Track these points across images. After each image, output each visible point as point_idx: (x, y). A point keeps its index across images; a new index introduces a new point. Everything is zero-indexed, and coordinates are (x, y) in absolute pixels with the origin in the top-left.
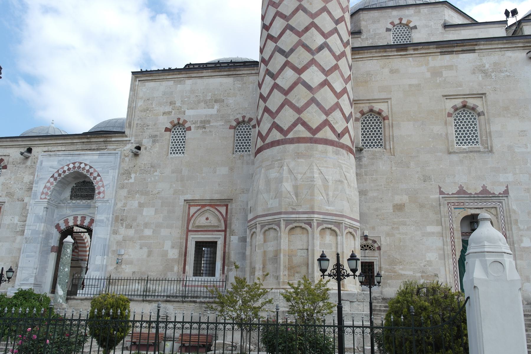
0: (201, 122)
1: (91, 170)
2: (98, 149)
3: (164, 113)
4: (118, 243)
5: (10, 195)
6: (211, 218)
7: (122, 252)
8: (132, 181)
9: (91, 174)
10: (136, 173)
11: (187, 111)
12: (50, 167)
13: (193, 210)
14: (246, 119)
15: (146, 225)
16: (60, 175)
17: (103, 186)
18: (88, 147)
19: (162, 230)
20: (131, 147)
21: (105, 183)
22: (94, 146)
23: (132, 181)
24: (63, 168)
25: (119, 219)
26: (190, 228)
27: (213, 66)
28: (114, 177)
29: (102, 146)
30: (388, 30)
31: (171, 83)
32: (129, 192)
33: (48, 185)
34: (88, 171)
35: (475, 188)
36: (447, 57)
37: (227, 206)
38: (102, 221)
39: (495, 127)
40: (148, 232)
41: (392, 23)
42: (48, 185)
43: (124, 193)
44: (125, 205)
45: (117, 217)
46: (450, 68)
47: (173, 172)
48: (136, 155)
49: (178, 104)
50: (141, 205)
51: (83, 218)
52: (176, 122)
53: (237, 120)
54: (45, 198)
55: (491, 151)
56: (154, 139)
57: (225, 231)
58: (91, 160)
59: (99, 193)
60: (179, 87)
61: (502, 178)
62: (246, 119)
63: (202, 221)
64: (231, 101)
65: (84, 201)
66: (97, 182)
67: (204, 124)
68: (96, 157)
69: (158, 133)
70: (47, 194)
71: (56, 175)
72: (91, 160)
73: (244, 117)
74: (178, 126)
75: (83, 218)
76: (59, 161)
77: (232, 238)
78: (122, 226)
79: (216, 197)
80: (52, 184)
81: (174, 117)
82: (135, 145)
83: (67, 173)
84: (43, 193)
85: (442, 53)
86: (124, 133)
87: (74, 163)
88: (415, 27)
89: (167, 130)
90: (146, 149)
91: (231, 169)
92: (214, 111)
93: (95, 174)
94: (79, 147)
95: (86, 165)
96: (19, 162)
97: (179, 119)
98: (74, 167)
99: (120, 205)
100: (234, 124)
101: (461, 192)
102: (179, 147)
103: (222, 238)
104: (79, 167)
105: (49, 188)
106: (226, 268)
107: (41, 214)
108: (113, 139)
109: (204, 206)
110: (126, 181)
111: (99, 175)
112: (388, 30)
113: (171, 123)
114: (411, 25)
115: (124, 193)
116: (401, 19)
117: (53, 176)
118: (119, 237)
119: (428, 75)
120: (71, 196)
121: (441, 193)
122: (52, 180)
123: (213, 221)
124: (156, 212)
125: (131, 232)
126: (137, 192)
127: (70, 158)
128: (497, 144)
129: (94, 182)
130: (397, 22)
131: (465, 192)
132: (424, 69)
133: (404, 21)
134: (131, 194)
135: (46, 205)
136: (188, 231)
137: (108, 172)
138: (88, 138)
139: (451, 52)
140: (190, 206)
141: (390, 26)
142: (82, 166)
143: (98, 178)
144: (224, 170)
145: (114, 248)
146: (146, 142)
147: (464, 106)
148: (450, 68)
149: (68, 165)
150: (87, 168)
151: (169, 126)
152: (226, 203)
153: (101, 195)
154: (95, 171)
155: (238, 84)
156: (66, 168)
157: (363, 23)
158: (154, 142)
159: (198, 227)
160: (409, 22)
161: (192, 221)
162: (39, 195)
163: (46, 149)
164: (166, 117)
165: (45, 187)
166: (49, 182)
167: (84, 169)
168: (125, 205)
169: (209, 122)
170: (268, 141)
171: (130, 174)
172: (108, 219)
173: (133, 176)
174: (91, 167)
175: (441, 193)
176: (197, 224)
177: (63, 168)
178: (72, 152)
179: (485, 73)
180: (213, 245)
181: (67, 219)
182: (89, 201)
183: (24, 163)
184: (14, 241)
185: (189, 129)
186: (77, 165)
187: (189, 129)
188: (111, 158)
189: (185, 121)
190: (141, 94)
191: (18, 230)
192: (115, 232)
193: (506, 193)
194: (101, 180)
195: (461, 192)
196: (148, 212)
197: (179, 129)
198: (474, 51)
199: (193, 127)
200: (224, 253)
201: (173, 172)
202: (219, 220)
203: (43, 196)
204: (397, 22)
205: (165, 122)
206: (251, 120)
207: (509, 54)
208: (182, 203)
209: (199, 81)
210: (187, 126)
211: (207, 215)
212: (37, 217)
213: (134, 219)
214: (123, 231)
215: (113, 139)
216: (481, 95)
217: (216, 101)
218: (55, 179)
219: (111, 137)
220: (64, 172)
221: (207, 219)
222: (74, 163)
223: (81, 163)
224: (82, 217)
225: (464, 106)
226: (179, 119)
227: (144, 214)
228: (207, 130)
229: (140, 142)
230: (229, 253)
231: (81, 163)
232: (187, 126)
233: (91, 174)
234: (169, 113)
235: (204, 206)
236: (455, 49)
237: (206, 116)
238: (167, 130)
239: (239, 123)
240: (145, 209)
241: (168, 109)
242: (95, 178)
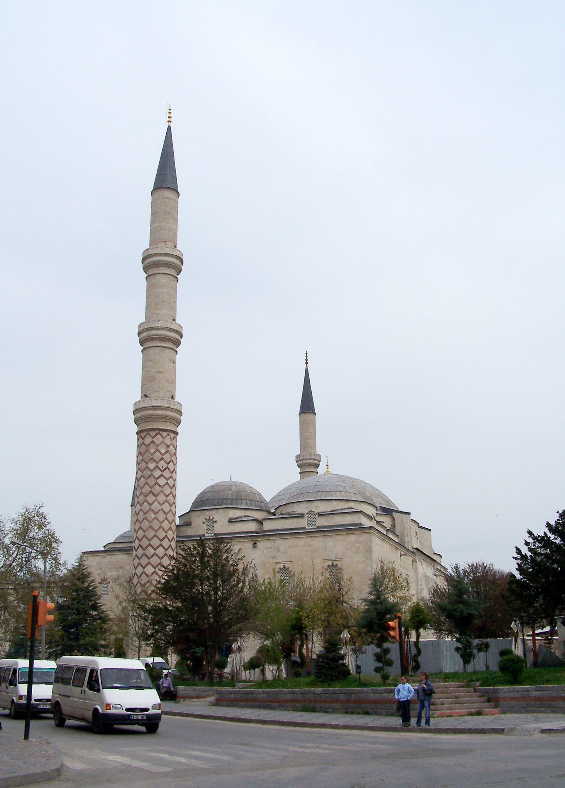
30: (204, 523)
41: (206, 519)
49: (104, 570)
60: (104, 560)
81: (102, 576)
88: (216, 522)
112: (204, 523)
114: (214, 520)
116: (210, 517)
130: (208, 518)
133: (211, 518)
141: (205, 521)
151: (100, 581)
157: (193, 518)
160: (213, 518)
187: (109, 583)
189: (107, 579)
199: (111, 582)
204: (208, 518)
207: (245, 544)
209: (113, 557)
210: (108, 581)
217: (121, 568)
232: (108, 581)
241: (99, 572)
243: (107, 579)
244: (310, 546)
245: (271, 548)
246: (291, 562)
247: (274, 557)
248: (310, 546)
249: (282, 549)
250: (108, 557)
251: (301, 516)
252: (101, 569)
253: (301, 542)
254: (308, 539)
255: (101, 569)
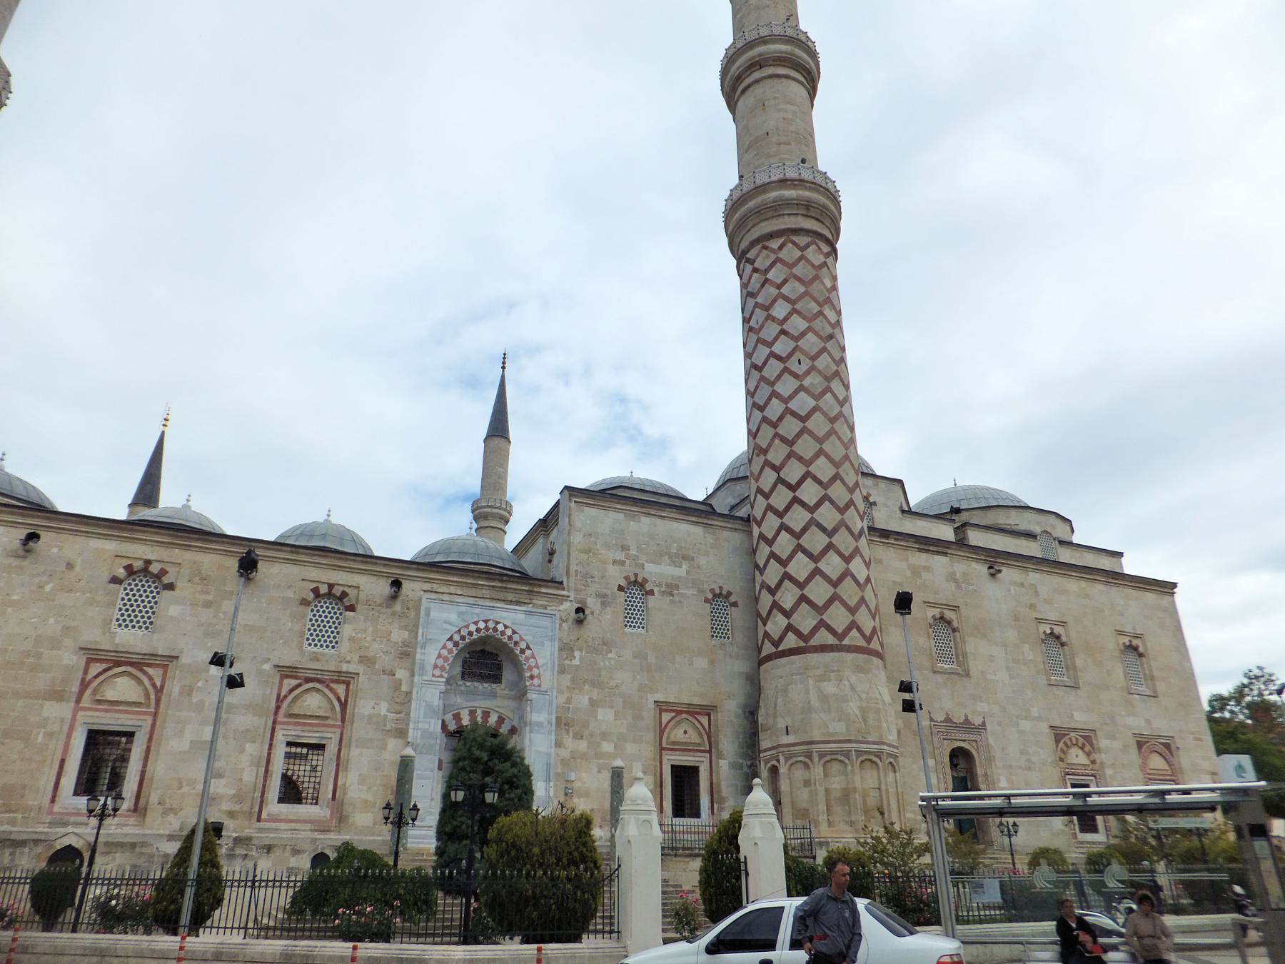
0: (667, 585)
1: (516, 638)
2: (518, 603)
3: (614, 562)
4: (564, 762)
5: (366, 660)
6: (690, 731)
7: (573, 776)
8: (576, 662)
9: (516, 643)
10: (581, 650)
11: (647, 565)
12: (446, 622)
13: (666, 717)
14: (724, 592)
15: (604, 736)
16: (463, 638)
17: (537, 666)
18: (501, 596)
19: (627, 745)
20: (568, 607)
21: (540, 662)
22: (511, 597)
23: (576, 662)
24: (467, 626)
25: (563, 723)
26: (664, 745)
27: (677, 503)
28: (552, 654)
29: (525, 598)
31: (621, 516)
32: (573, 680)
33: (445, 652)
34: (510, 638)
35: (959, 718)
36: (924, 555)
37: (709, 715)
38: (540, 725)
39: (969, 648)
40: (607, 747)
42: (445, 652)
43: (566, 680)
44: (569, 701)
45: (558, 719)
46: (927, 569)
47: (635, 657)
48: (580, 622)
49: (633, 551)
50: (593, 703)
51: (486, 714)
52: (633, 579)
53: (712, 590)
54: (441, 676)
55: (968, 675)
56: (604, 599)
57: (710, 752)
58: (511, 619)
59: (532, 677)
61: (983, 707)
62: (724, 592)
63: (678, 734)
64: (703, 561)
65: (486, 685)
66: (527, 659)
67: (671, 589)
68: (521, 617)
69: (609, 592)
70: (443, 668)
71: (457, 638)
72: (511, 619)
73: (721, 588)
74: (637, 585)
75: (486, 714)
76: (460, 614)
77: (722, 762)
78: (568, 731)
79: (696, 701)
80: (450, 651)
81: (629, 570)
82: (577, 605)
83: (475, 636)
84: (436, 666)
85: (920, 550)
86: (561, 583)
87: (486, 621)
89: (621, 588)
90: (592, 613)
91: (712, 662)
92: (682, 572)
93: (523, 645)
94: (486, 593)
95: (506, 627)
96: (379, 602)
97: (636, 575)
98: (487, 628)
99: (562, 699)
100: (710, 596)
101: (948, 720)
102: (632, 618)
103: (707, 761)
104: (495, 630)
105: (446, 659)
106: (716, 806)
107: (436, 703)
108: (543, 590)
109: (679, 713)
110: (567, 662)
111: (528, 648)
113: (626, 578)
115: (566, 680)
117: (451, 639)
118: (565, 753)
119: (909, 573)
120: (463, 673)
121: (932, 720)
122: (450, 645)
123: (693, 737)
124: (617, 716)
125: (582, 746)
126: (585, 681)
127: (477, 611)
128: (974, 666)
129: (522, 658)
131: (951, 722)
132: (904, 565)
134: (576, 684)
135: (443, 688)
136: (662, 749)
137: (542, 644)
138: (502, 581)
139: (927, 551)
140: (661, 711)
142: (501, 627)
143: (528, 652)
144: (702, 663)
145: (559, 771)
146: (592, 603)
147: (942, 618)
148: (927, 569)
149: (476, 623)
150: (509, 632)
151: (623, 583)
152: (708, 710)
153: (536, 681)
154: (522, 639)
155: (710, 540)
156: (473, 628)
158: (604, 604)
159: (674, 743)
161: (666, 735)
162: (429, 668)
163: (427, 586)
164: (617, 568)
165: (439, 656)
166: (444, 647)
167: (503, 633)
168: (569, 701)
169: (677, 587)
170: (813, 642)
171: (572, 650)
172: (549, 722)
173: (577, 654)
174: (514, 632)
175: (932, 720)
176: (673, 739)
177: (467, 626)
178: (481, 602)
179: (956, 581)
180: (694, 771)
181: (459, 714)
182: (494, 686)
183: (387, 607)
184: (384, 747)
185: (651, 593)
186: (491, 625)
187: (651, 593)
188: (546, 622)
189: (645, 581)
190: (578, 524)
191: (388, 727)
192: (558, 744)
193: (984, 723)
194: (533, 656)
195: (948, 720)
196: (605, 716)
197: (635, 591)
198: (945, 554)
199: (656, 590)
200: (711, 784)
201: (635, 657)
202: (702, 737)
203: (437, 672)
205: (616, 576)
206: (729, 594)
207: (974, 565)
208: (652, 706)
209: (659, 522)
210: (648, 587)
211: (685, 726)
212: (429, 706)
213: (586, 725)
214: (569, 741)
215: (543, 590)
216: (955, 608)
217: (684, 558)
218: (456, 644)
219: (540, 586)
220: (470, 633)
221: (685, 732)
222: (486, 621)
223: (497, 623)
224: (484, 712)
225: (942, 618)
226: (636, 575)
227: (600, 717)
228: (677, 599)
229: (583, 601)
230: (719, 785)
231: (497, 623)
232: (648, 587)
233: (516, 643)
234: (622, 563)
235: (679, 713)
236: (931, 548)
237: (673, 577)
238: (621, 588)
239: (715, 596)
240: (600, 710)
241: (620, 556)
242: (523, 651)
243: (645, 581)
244: (1087, 596)
245: (1022, 585)
246: (1063, 624)
247: (1032, 606)
248: (1087, 596)
249: (1043, 590)
250: (646, 520)
251: (1031, 536)
252: (624, 548)
253: (1074, 585)
254: (1083, 584)
255: (624, 548)
